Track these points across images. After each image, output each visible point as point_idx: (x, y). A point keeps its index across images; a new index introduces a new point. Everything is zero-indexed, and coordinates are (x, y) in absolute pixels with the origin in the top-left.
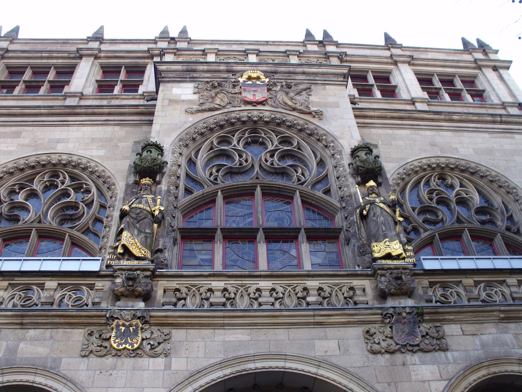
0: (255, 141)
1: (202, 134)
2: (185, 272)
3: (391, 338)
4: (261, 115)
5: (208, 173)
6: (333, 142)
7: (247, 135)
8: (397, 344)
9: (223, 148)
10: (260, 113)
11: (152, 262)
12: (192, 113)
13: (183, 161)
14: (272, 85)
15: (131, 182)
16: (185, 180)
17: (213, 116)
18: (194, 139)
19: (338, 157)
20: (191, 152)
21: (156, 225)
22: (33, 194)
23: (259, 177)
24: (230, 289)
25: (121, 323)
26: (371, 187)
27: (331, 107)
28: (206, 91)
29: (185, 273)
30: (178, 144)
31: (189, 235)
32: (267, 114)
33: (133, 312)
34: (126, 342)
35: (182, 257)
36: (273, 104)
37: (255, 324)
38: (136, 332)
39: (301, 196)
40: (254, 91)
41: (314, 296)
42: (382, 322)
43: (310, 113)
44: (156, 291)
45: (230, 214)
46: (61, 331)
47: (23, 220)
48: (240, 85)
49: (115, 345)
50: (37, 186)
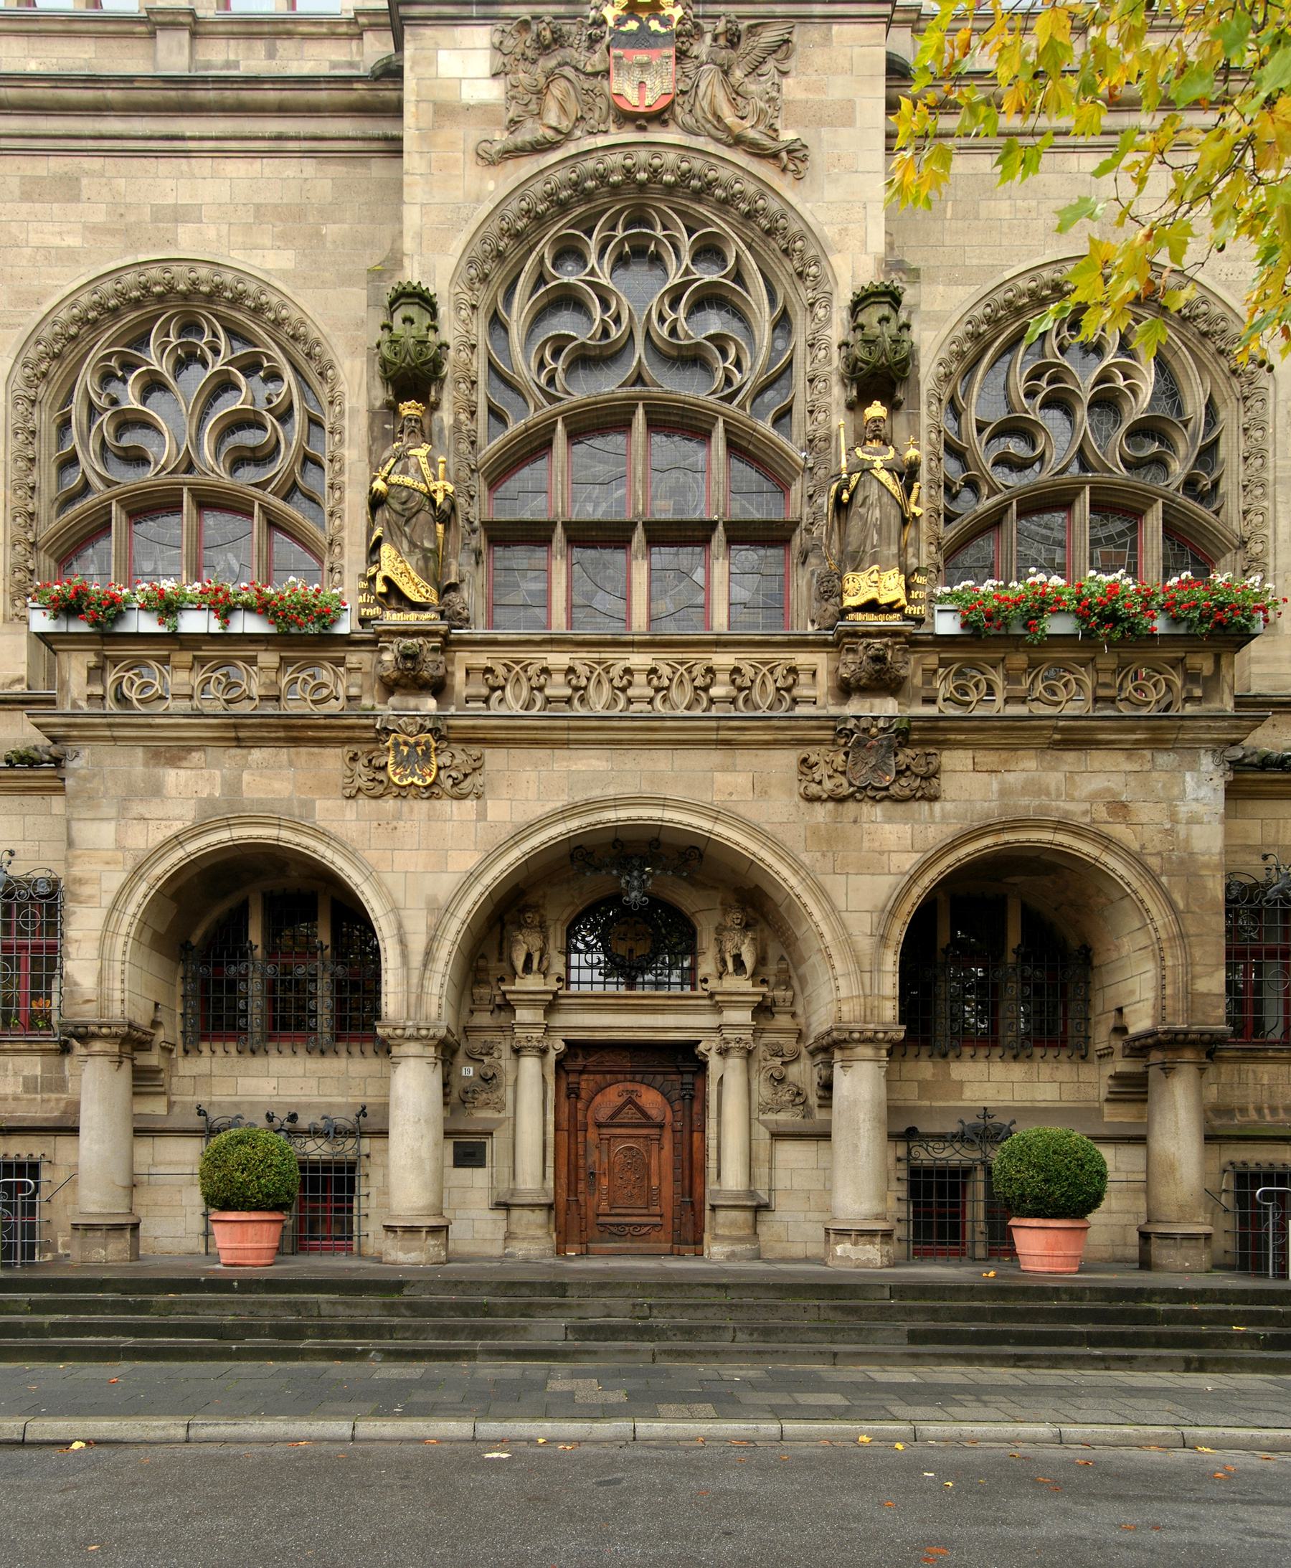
0: (638, 254)
1: (517, 236)
2: (501, 635)
3: (843, 773)
4: (656, 162)
5: (534, 365)
6: (817, 263)
7: (620, 233)
8: (851, 785)
9: (565, 280)
10: (656, 155)
11: (442, 615)
12: (492, 163)
13: (479, 329)
14: (689, 35)
15: (378, 404)
16: (489, 385)
17: (541, 172)
18: (500, 256)
19: (821, 312)
20: (496, 295)
21: (440, 527)
22: (153, 384)
23: (647, 378)
24: (581, 669)
25: (402, 737)
26: (874, 420)
27: (832, 125)
28: (522, 66)
29: (500, 637)
30: (466, 277)
31: (505, 535)
32: (671, 157)
33: (419, 720)
34: (413, 774)
35: (493, 586)
36: (689, 120)
37: (619, 742)
38: (426, 754)
39: (726, 431)
40: (644, 66)
41: (724, 684)
42: (834, 742)
43: (775, 156)
44: (453, 674)
45: (582, 475)
46: (303, 750)
47: (156, 464)
48: (608, 38)
49: (396, 779)
50: (156, 360)
